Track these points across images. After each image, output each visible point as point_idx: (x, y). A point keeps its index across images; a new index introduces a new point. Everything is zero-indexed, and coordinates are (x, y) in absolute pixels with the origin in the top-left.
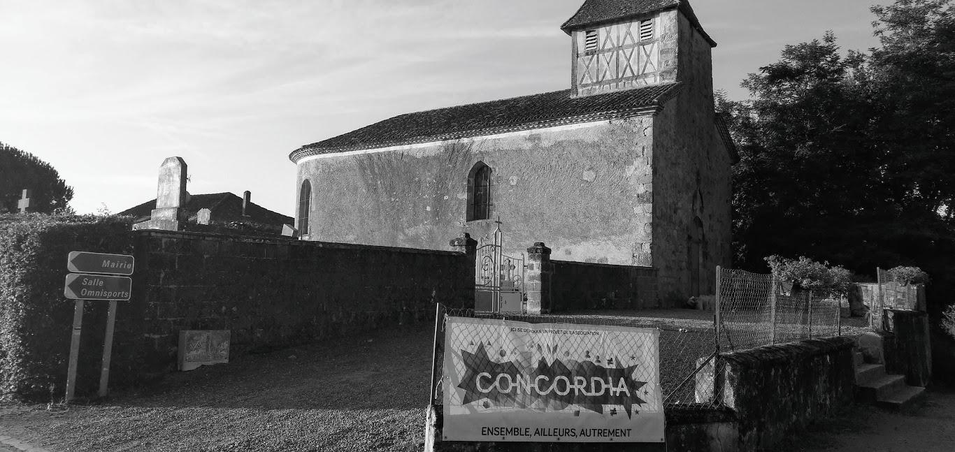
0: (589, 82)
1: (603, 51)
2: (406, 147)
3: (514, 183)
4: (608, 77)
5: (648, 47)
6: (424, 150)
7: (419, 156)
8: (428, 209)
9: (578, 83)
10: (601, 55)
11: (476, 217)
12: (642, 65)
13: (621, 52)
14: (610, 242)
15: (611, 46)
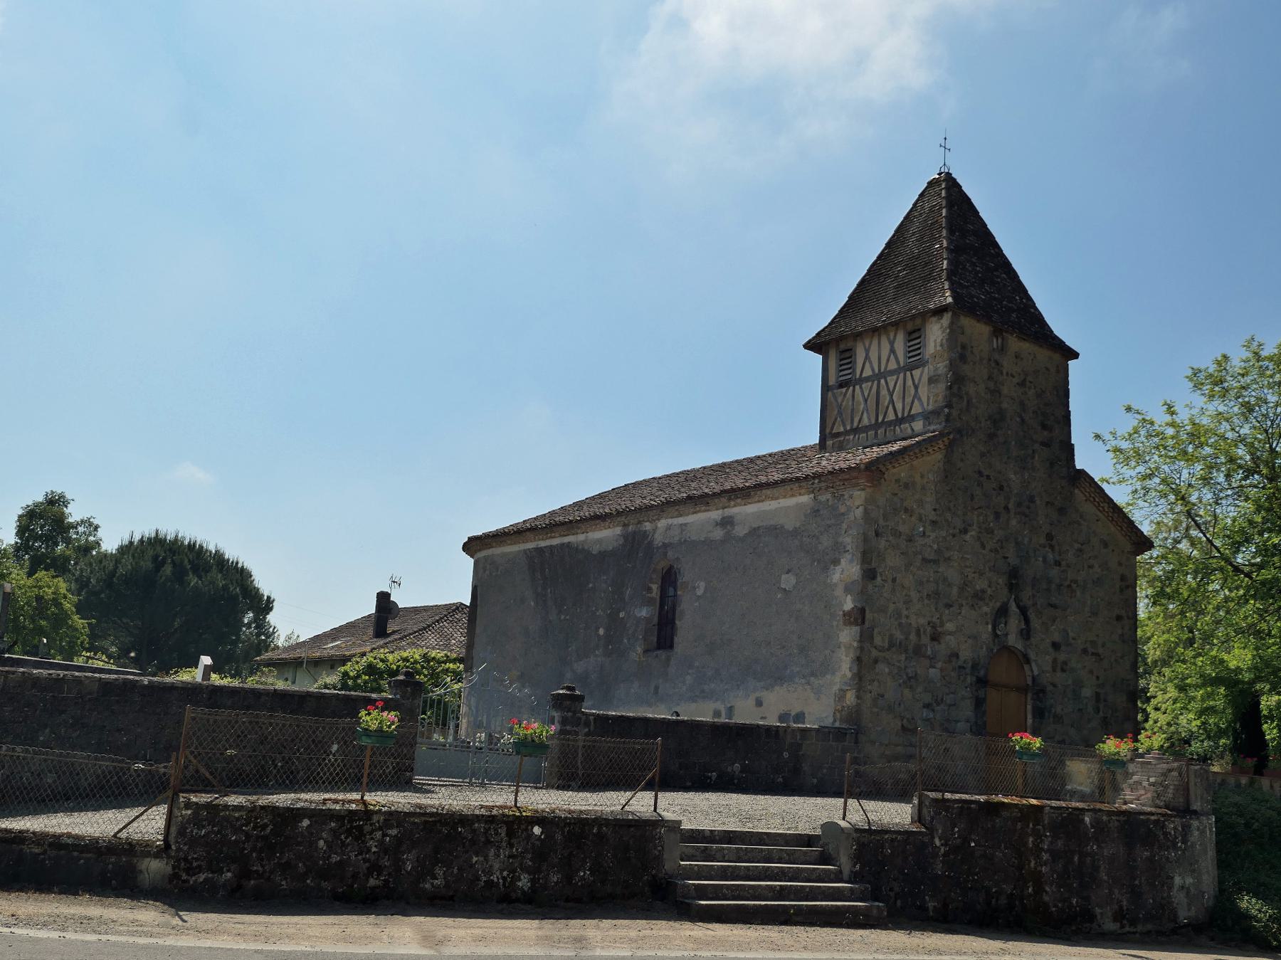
0: (842, 429)
1: (861, 380)
2: (581, 537)
3: (700, 592)
4: (866, 421)
5: (917, 373)
6: (600, 541)
7: (595, 550)
8: (601, 632)
9: (828, 431)
10: (857, 387)
11: (660, 646)
12: (908, 400)
13: (883, 381)
14: (807, 687)
15: (870, 373)
